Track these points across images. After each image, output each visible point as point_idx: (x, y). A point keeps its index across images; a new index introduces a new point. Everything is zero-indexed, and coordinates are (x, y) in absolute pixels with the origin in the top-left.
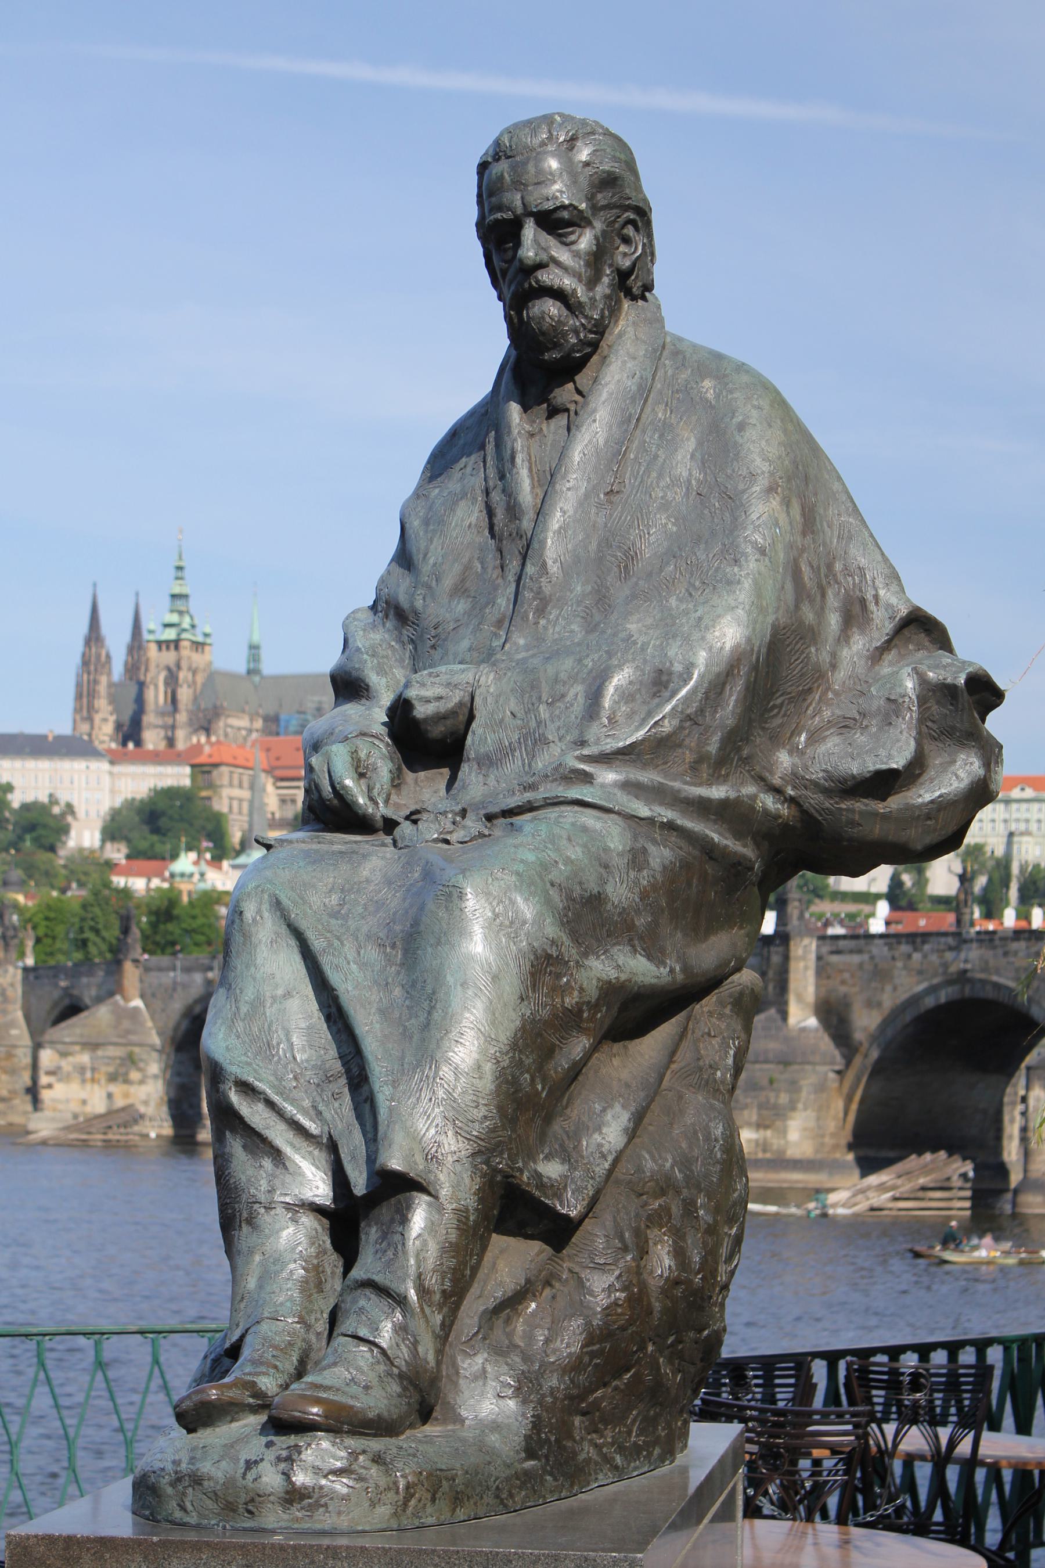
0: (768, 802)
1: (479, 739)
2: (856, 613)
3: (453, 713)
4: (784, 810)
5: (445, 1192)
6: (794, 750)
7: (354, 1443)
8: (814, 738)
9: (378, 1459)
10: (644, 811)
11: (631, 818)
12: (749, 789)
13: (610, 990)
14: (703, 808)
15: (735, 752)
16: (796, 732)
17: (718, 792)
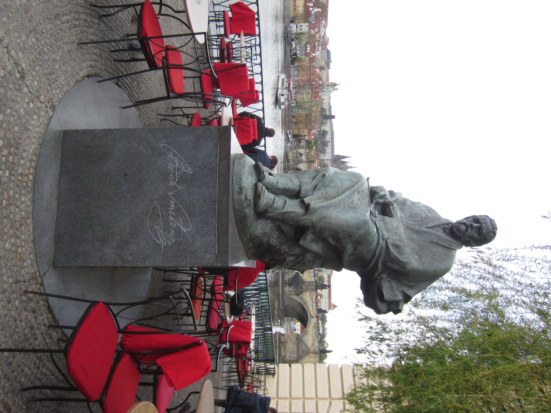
0: (377, 274)
1: (387, 219)
2: (411, 287)
3: (391, 214)
4: (375, 276)
5: (305, 217)
6: (386, 278)
7: (252, 201)
8: (389, 282)
9: (249, 205)
10: (377, 252)
11: (376, 250)
12: (380, 271)
13: (344, 248)
14: (377, 263)
15: (386, 268)
16: (390, 278)
17: (380, 265)
